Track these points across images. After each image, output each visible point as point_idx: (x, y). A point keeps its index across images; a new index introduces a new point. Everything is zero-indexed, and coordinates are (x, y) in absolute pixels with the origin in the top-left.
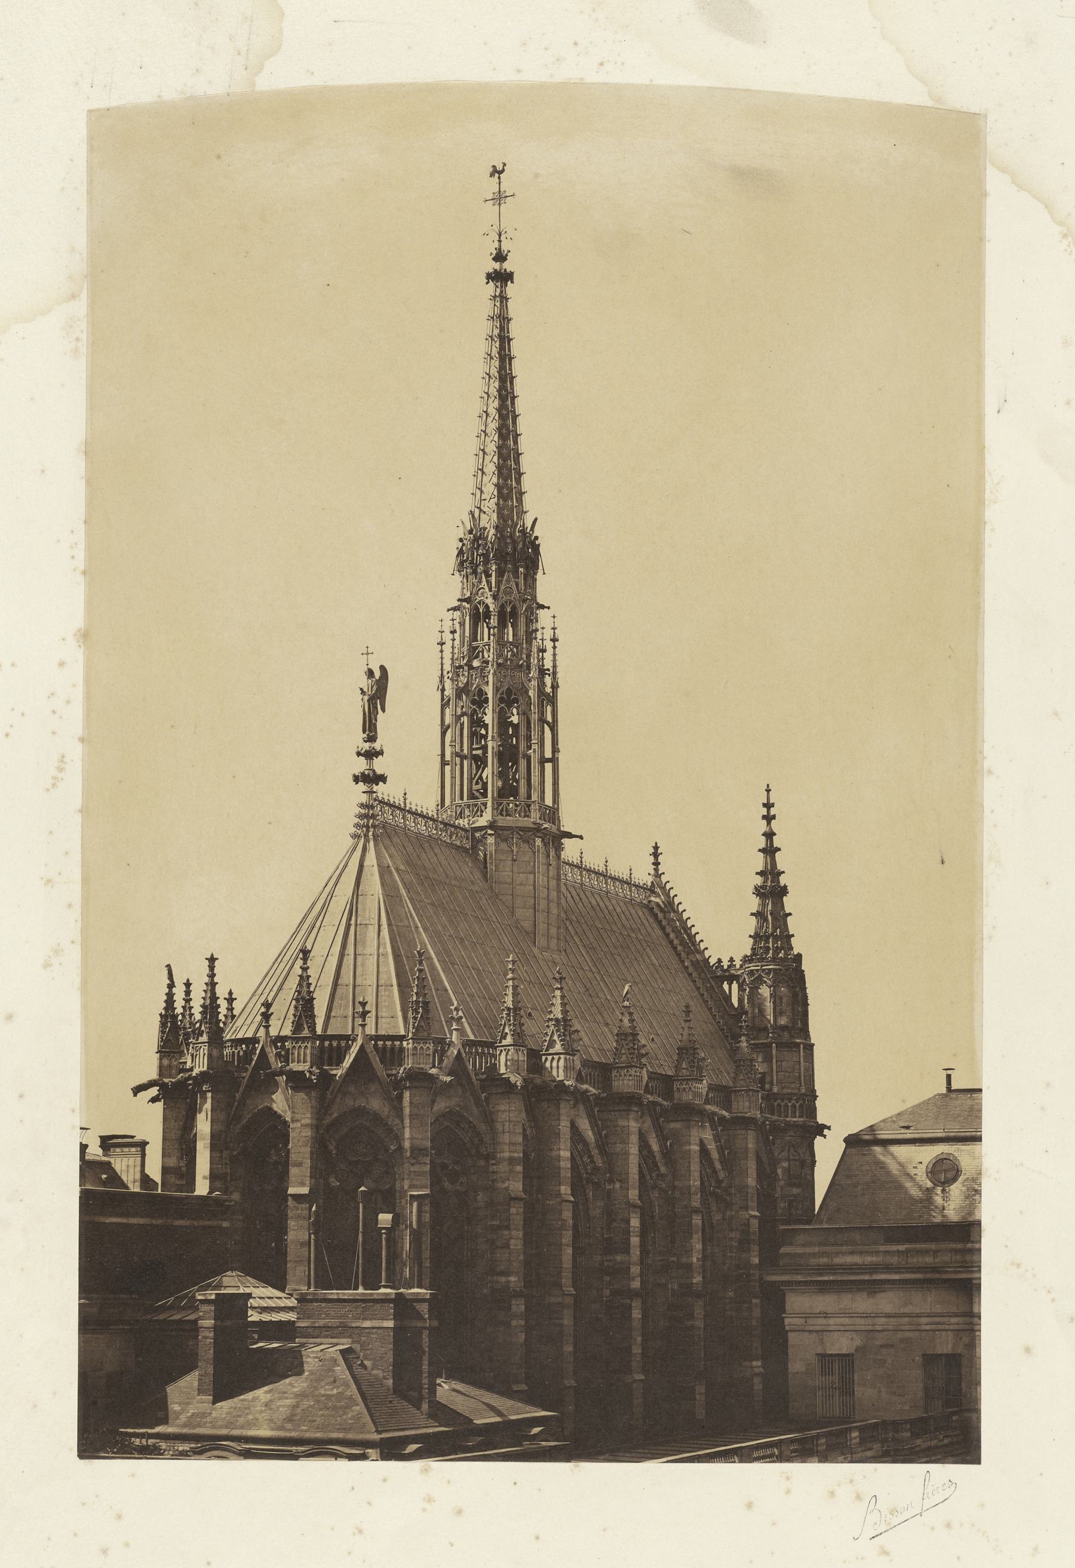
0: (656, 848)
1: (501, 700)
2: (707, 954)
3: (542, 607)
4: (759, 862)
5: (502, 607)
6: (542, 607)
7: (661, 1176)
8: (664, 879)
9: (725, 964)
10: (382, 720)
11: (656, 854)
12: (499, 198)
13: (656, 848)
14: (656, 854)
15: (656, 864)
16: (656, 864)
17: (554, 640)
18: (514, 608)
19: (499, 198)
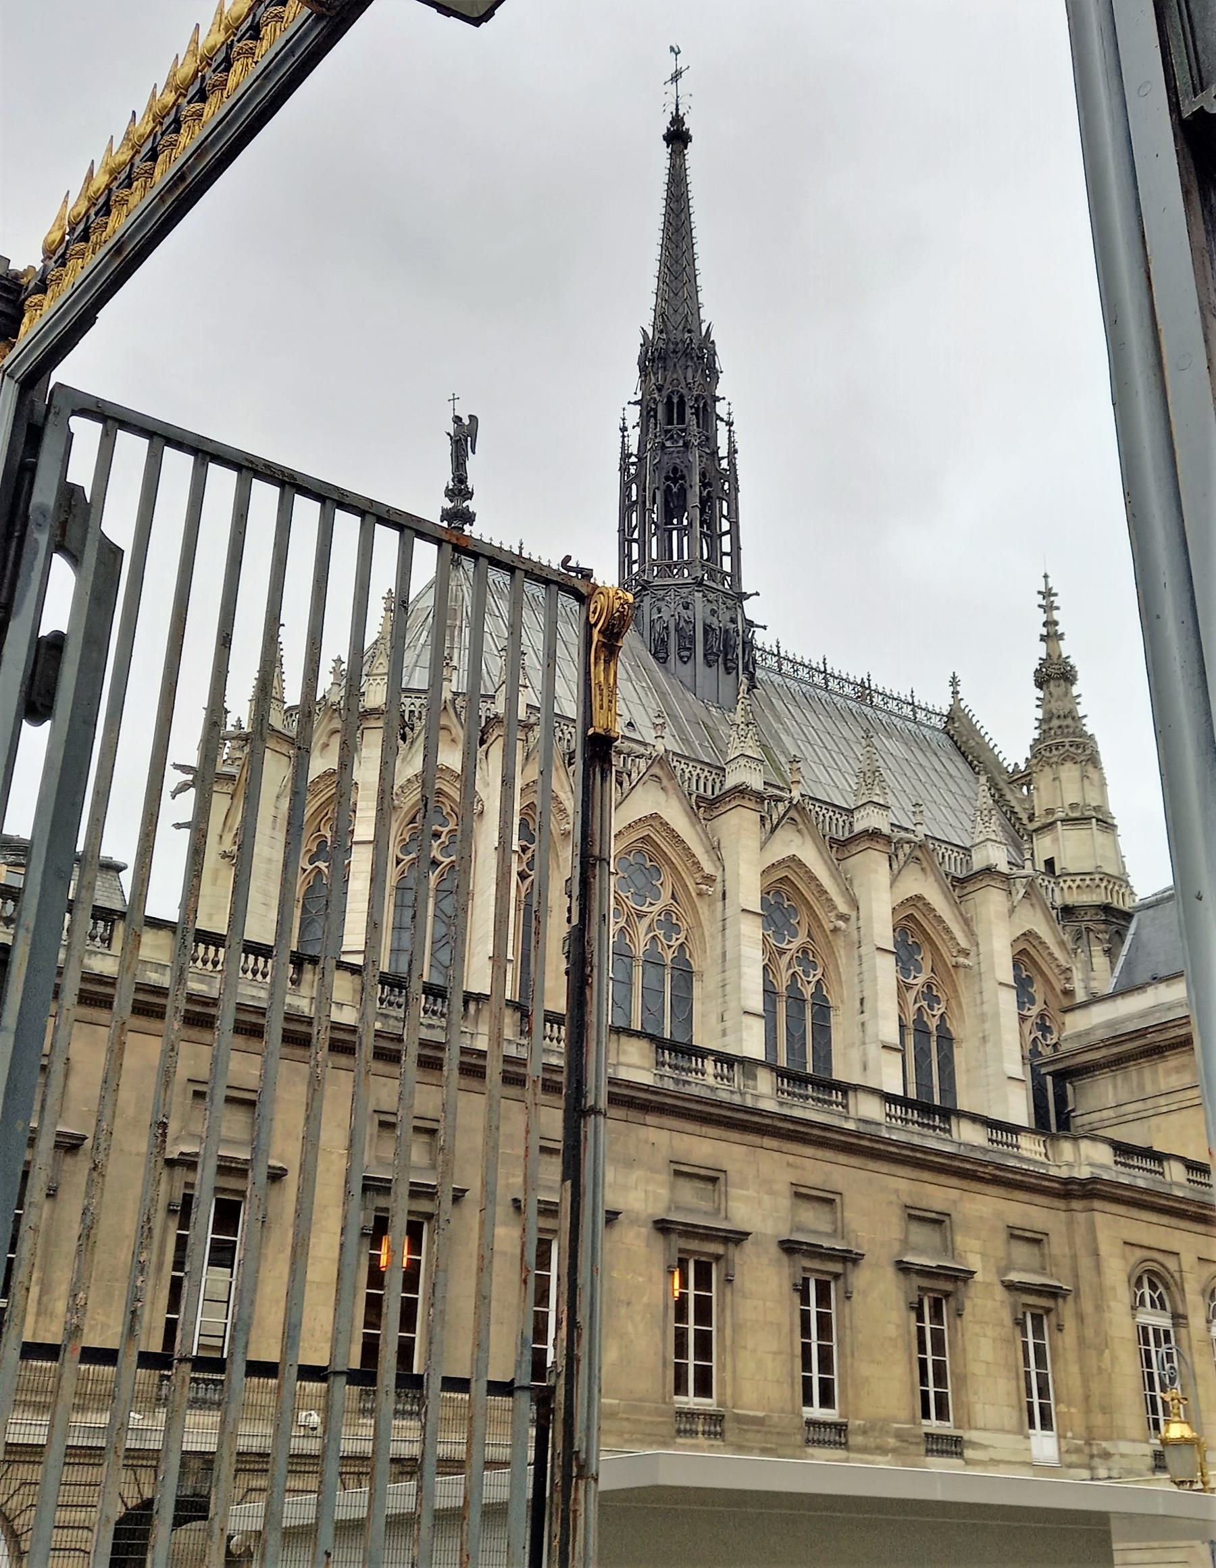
0: (954, 678)
1: (667, 478)
2: (1005, 765)
3: (718, 399)
4: (1041, 650)
5: (670, 398)
6: (718, 399)
7: (844, 917)
8: (963, 705)
9: (1022, 767)
10: (473, 464)
11: (954, 682)
12: (676, 76)
13: (954, 678)
14: (954, 682)
15: (955, 693)
16: (955, 693)
17: (729, 424)
18: (681, 397)
19: (676, 76)
